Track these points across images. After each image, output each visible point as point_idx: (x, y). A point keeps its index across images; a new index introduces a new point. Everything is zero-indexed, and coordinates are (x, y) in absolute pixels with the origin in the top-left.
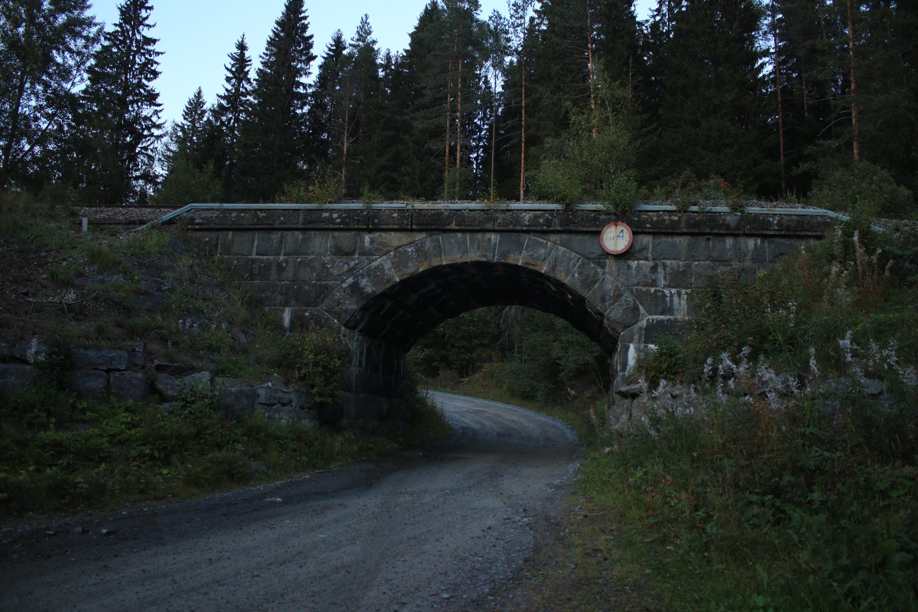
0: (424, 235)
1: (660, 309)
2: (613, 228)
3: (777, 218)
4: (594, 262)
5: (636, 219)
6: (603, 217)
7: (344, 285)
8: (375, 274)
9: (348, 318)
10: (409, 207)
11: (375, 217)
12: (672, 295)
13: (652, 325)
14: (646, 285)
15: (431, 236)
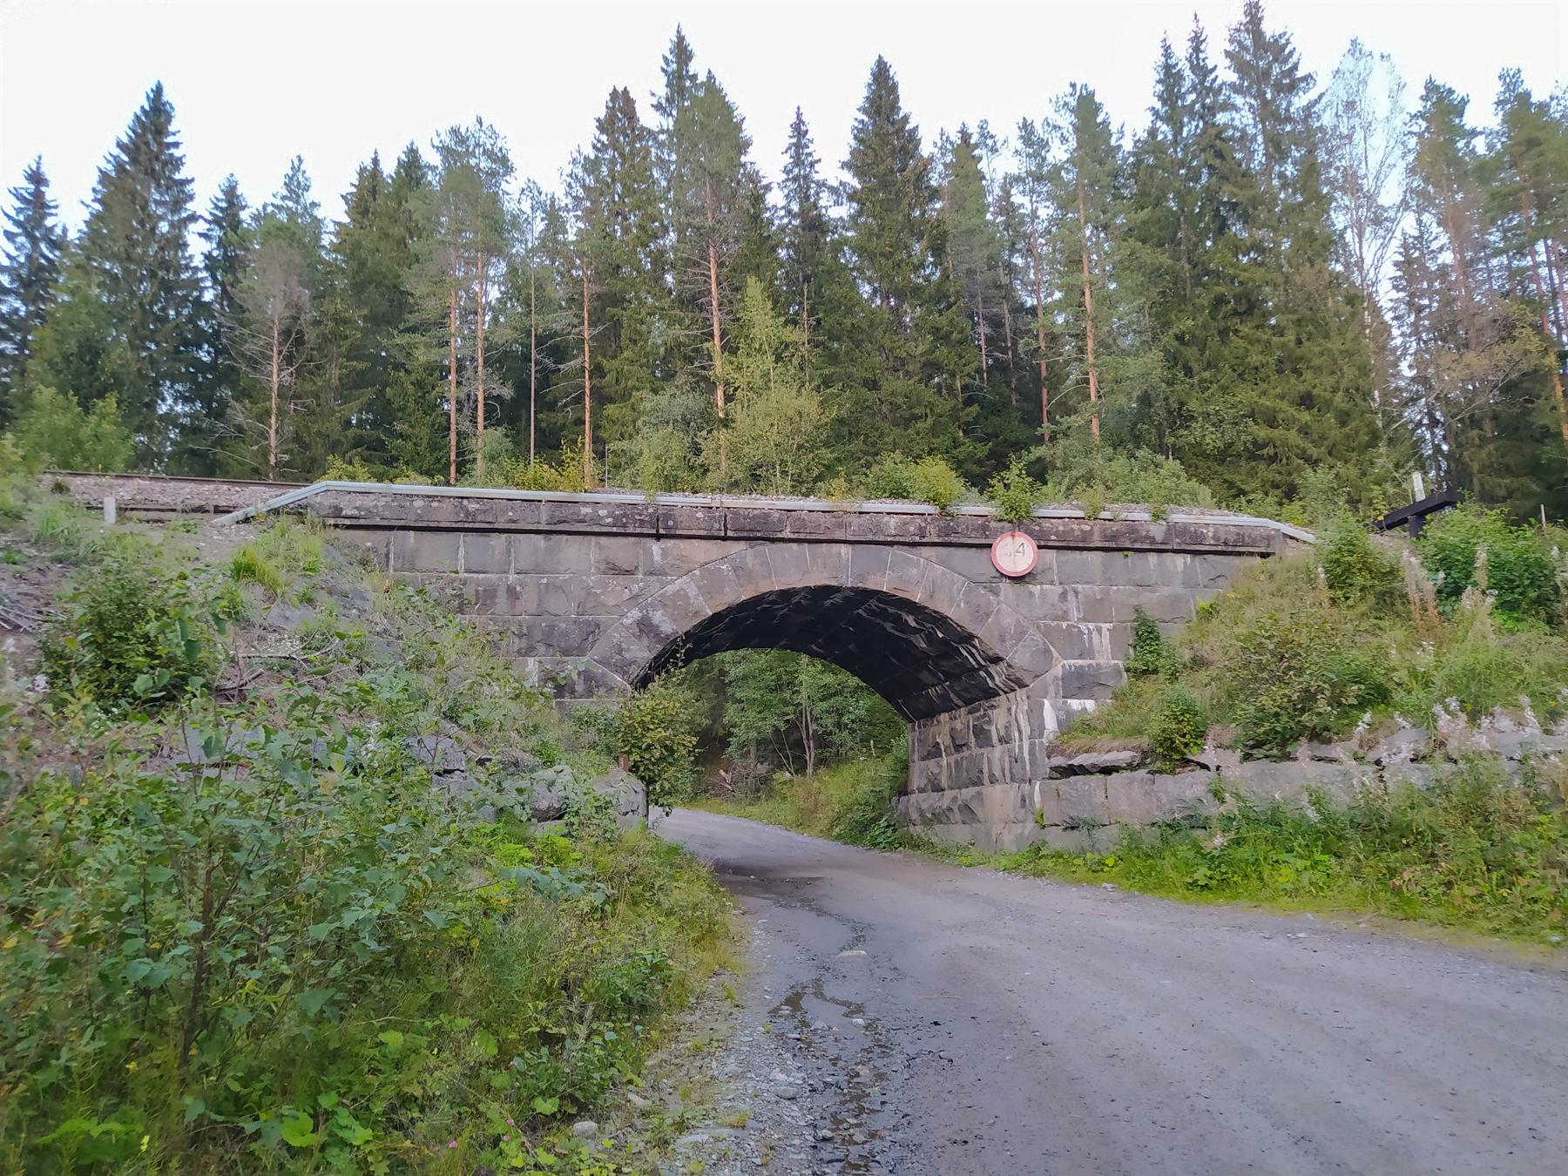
0: (742, 545)
2: (1009, 539)
6: (993, 524)
7: (627, 622)
11: (668, 517)
12: (1090, 633)
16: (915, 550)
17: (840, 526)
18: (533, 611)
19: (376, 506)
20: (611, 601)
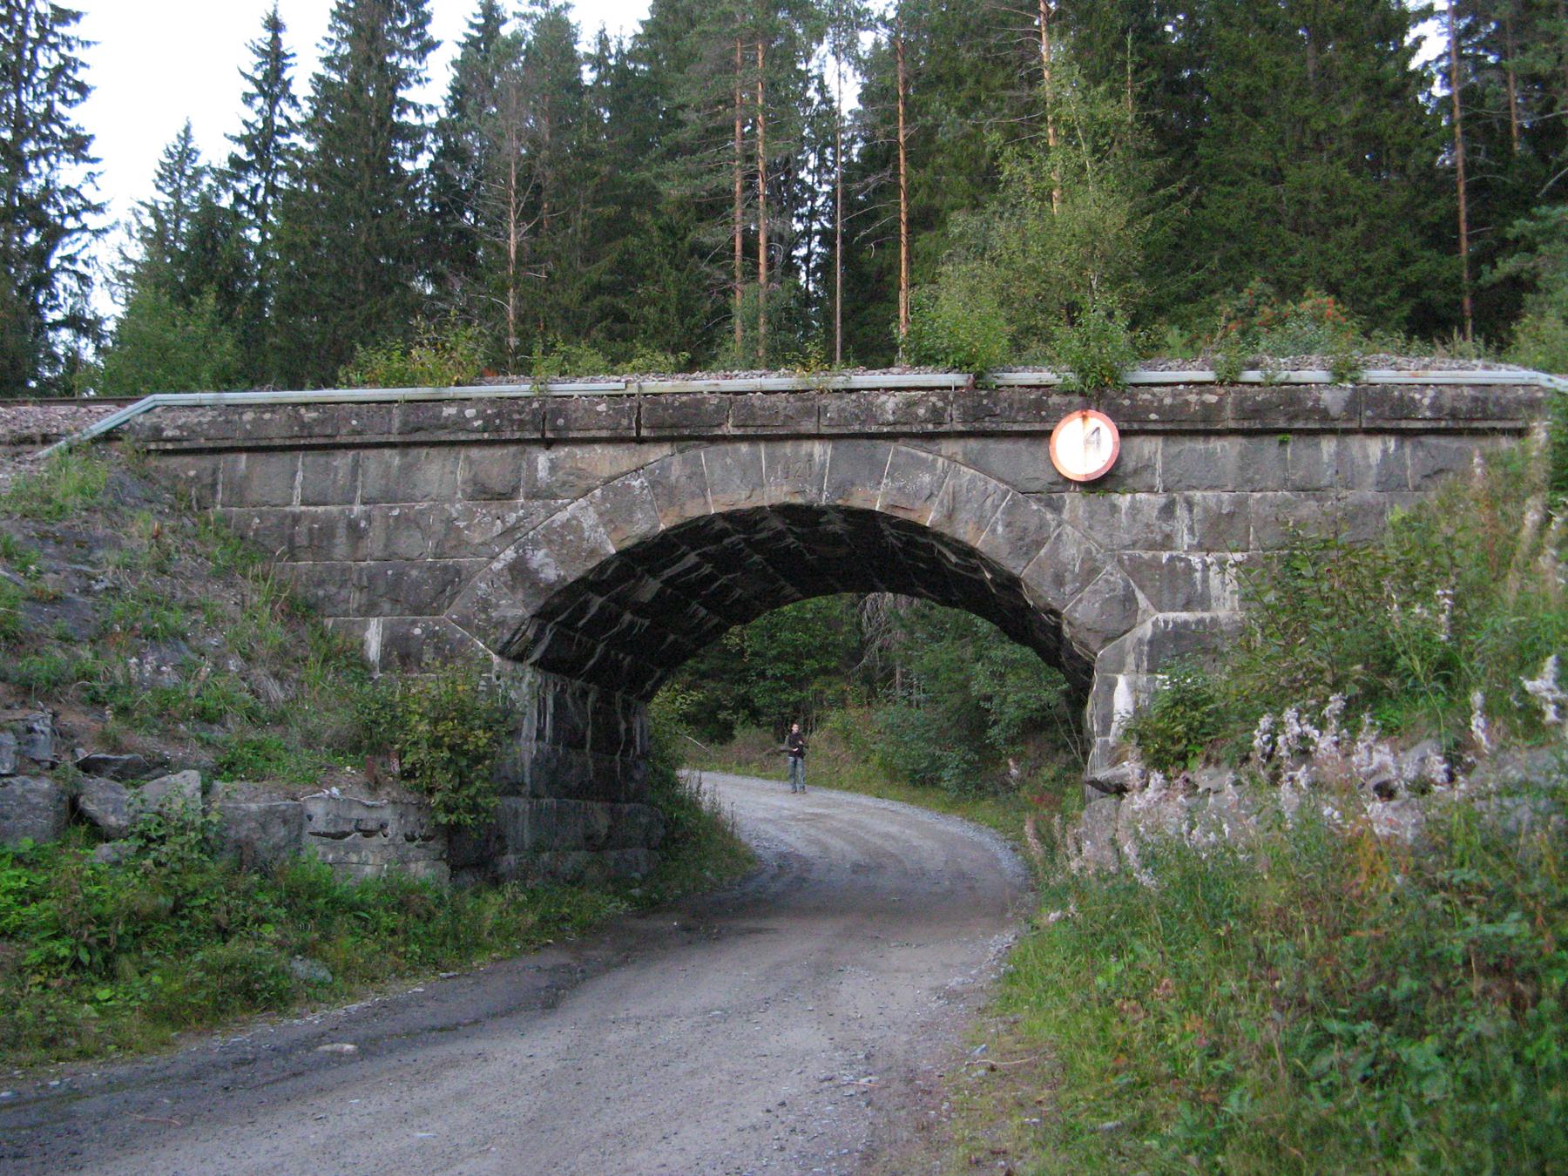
0: (666, 449)
1: (1181, 598)
3: (1430, 393)
4: (1039, 500)
5: (1127, 402)
6: (1055, 399)
7: (497, 566)
8: (563, 539)
9: (507, 637)
10: (633, 389)
11: (557, 413)
12: (1206, 567)
13: (1165, 634)
14: (1152, 546)
15: (681, 452)
16: (931, 446)
17: (808, 413)
18: (377, 554)
19: (200, 423)
20: (477, 538)
